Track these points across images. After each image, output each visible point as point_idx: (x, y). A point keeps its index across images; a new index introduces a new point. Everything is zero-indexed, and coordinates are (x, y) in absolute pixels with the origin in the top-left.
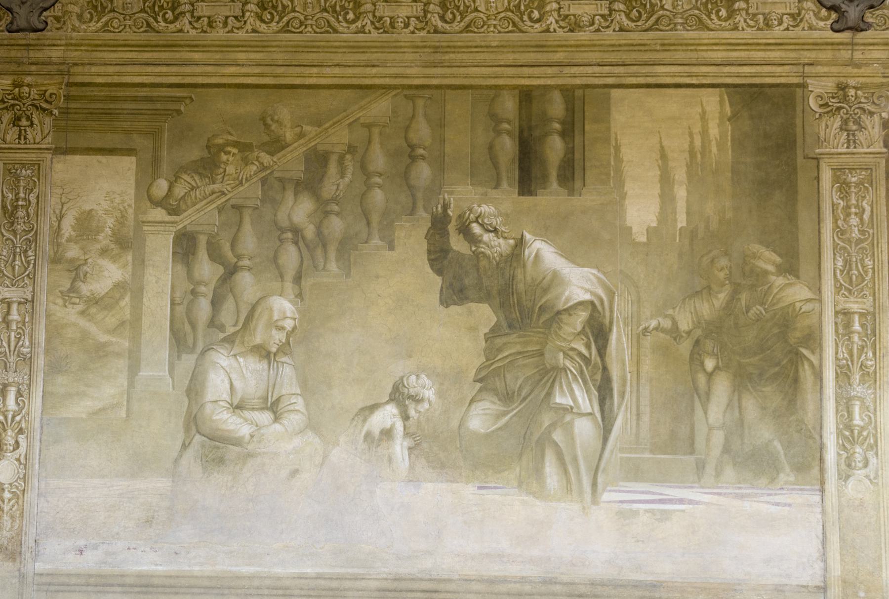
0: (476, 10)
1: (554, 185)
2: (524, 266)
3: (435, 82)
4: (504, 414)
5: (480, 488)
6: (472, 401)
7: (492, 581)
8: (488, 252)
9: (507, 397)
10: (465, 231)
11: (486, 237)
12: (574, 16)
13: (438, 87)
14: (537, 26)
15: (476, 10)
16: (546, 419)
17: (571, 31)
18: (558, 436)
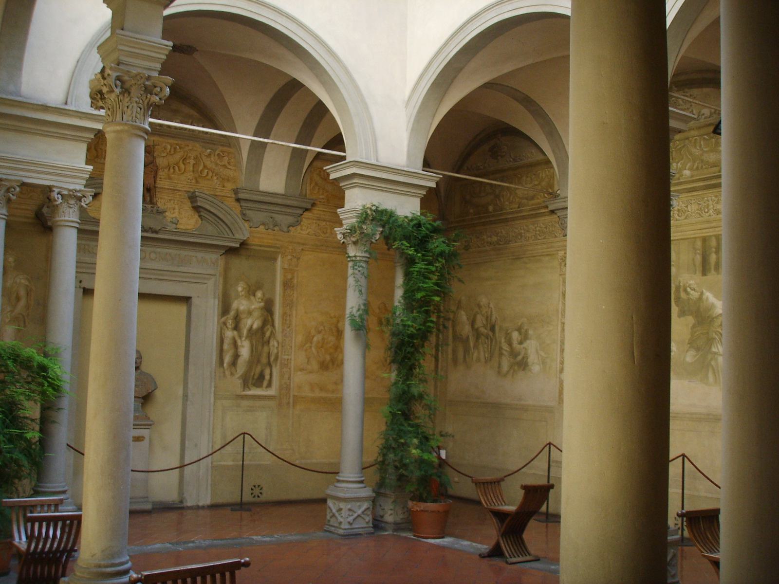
0: (688, 211)
1: (713, 271)
2: (703, 302)
3: (677, 238)
4: (696, 355)
5: (689, 381)
6: (687, 351)
7: (692, 414)
8: (692, 297)
9: (698, 349)
10: (685, 291)
11: (692, 292)
12: (718, 209)
13: (677, 240)
14: (707, 214)
15: (688, 211)
16: (710, 356)
17: (717, 215)
18: (713, 363)
